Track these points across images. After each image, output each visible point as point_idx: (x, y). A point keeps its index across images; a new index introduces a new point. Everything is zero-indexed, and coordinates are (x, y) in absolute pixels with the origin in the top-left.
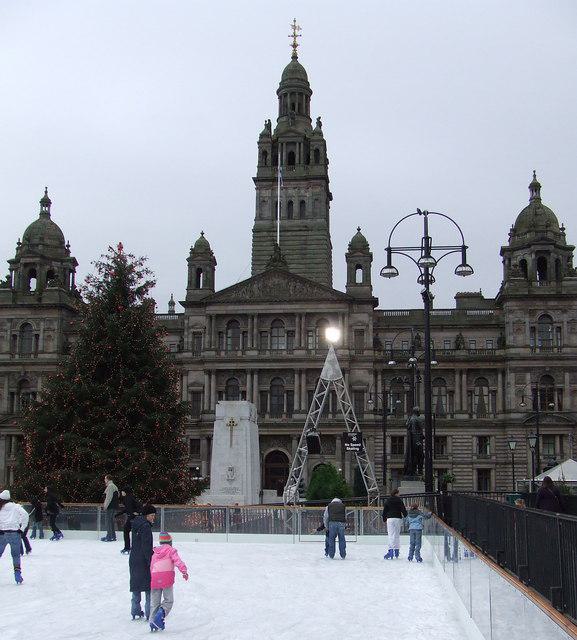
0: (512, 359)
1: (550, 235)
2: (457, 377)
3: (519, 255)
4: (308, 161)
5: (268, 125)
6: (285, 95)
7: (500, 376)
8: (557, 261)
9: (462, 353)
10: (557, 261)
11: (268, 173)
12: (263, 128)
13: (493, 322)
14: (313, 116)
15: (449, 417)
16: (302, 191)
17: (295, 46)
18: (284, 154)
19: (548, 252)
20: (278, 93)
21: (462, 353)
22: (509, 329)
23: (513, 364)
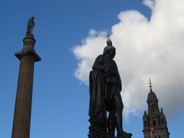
4: (160, 123)
5: (145, 112)
6: (150, 102)
11: (147, 128)
12: (143, 114)
14: (160, 108)
16: (159, 133)
17: (151, 86)
18: (152, 122)
20: (147, 102)
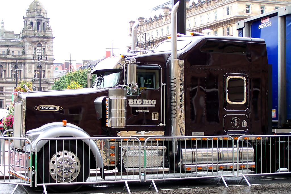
0: (27, 59)
1: (42, 14)
2: (8, 65)
3: (31, 20)
7: (23, 65)
8: (44, 23)
9: (9, 56)
10: (44, 23)
13: (21, 45)
15: (4, 80)
19: (41, 20)
21: (9, 56)
22: (26, 48)
23: (28, 61)
